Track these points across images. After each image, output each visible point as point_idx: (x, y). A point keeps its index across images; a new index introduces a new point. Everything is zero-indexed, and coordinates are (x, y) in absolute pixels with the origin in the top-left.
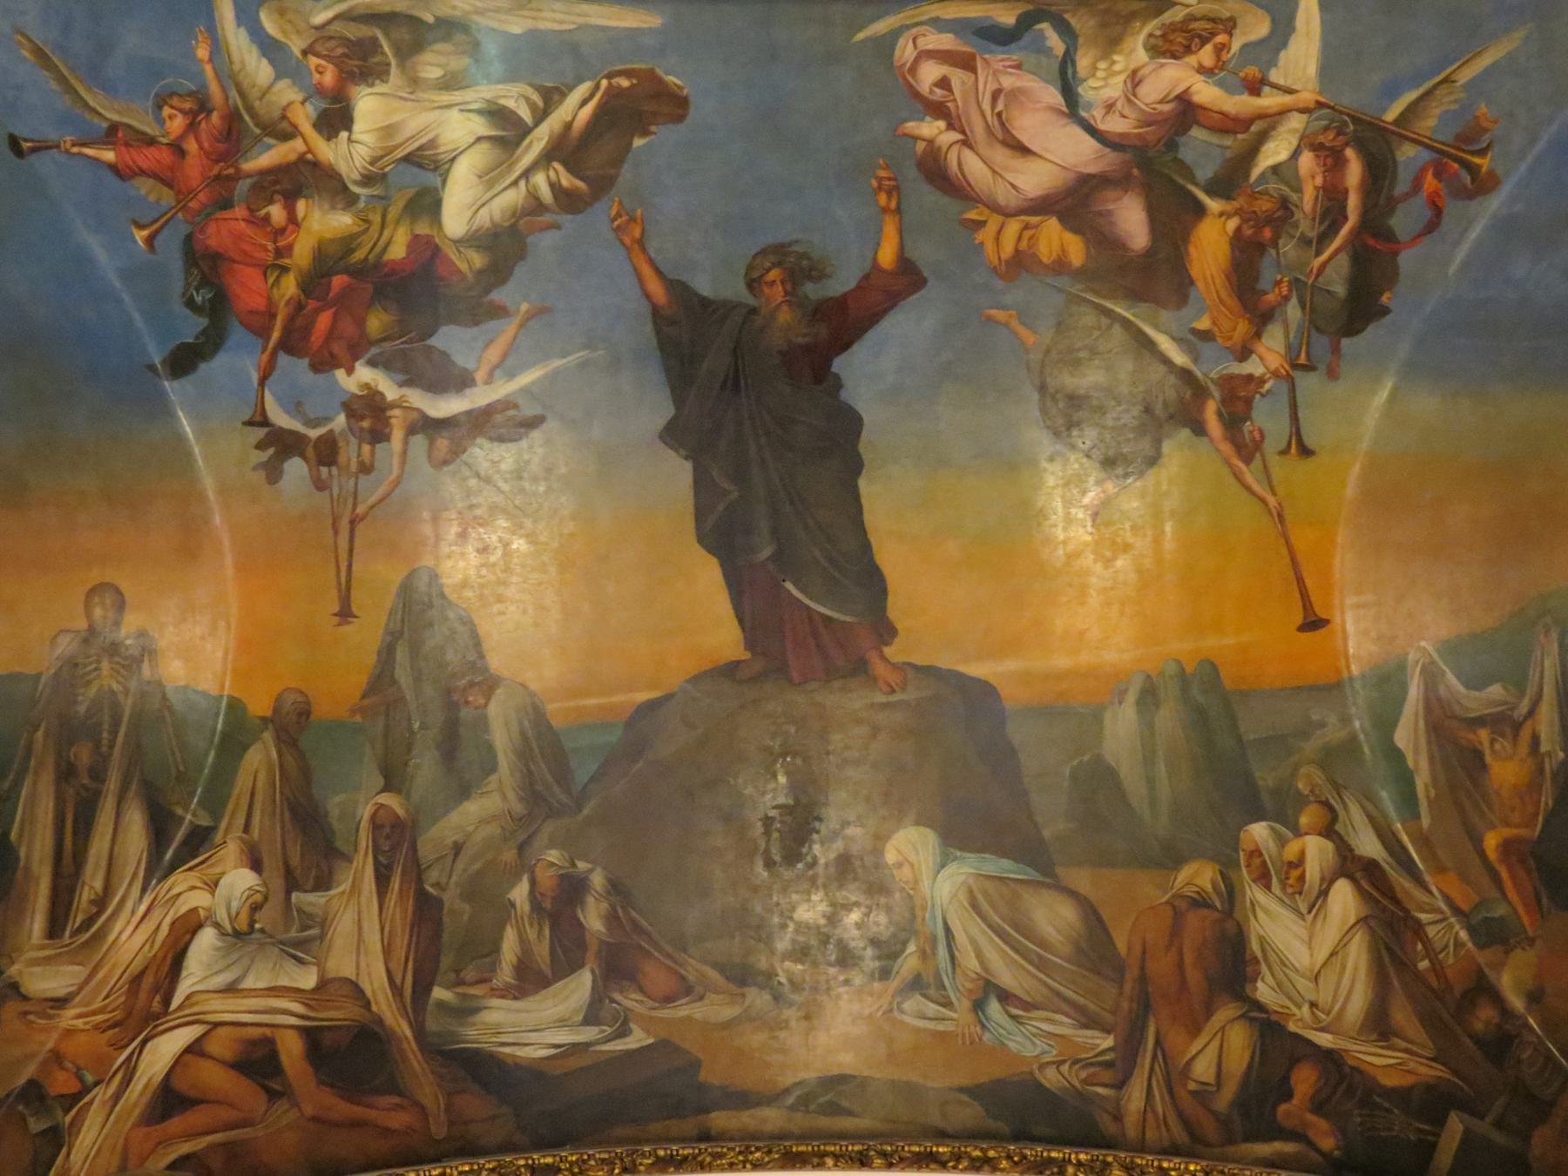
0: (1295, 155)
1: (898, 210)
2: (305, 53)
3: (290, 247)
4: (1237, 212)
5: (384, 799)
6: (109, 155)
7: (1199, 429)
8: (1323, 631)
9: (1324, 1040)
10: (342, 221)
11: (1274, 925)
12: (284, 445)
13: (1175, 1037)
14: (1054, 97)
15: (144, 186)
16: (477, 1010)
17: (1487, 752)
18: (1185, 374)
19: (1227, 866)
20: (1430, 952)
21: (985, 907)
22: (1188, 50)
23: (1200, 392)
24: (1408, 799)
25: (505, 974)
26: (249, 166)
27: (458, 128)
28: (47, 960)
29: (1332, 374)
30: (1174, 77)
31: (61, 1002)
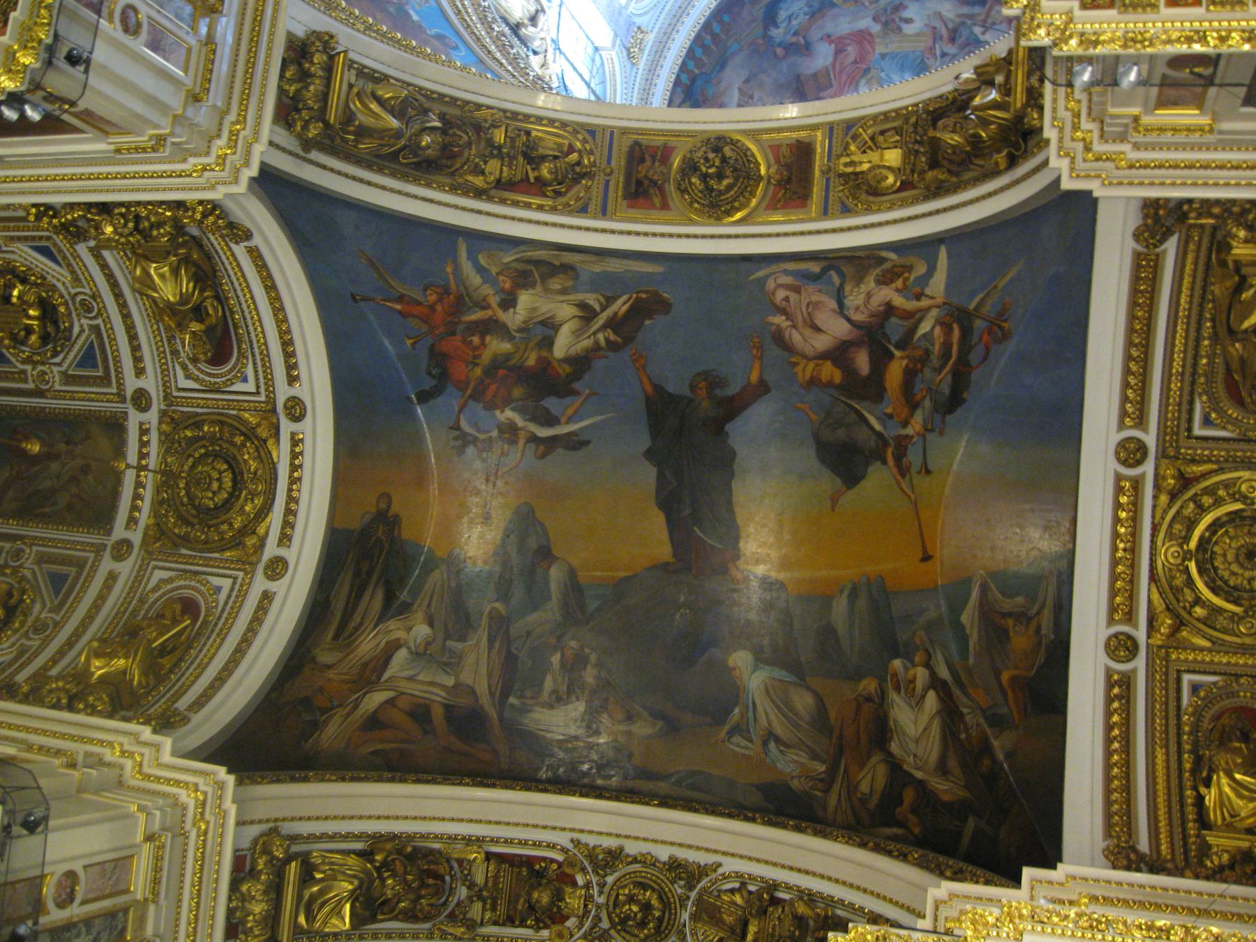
0: (933, 328)
1: (761, 358)
2: (498, 274)
3: (480, 356)
4: (908, 357)
5: (497, 605)
6: (399, 307)
7: (885, 462)
8: (929, 562)
9: (919, 775)
10: (506, 347)
14: (833, 304)
15: (413, 322)
16: (530, 711)
17: (1011, 629)
18: (879, 435)
19: (882, 680)
20: (967, 730)
21: (772, 693)
22: (892, 281)
23: (886, 444)
24: (964, 650)
27: (565, 311)
28: (329, 649)
29: (941, 433)
30: (888, 294)
31: (328, 667)
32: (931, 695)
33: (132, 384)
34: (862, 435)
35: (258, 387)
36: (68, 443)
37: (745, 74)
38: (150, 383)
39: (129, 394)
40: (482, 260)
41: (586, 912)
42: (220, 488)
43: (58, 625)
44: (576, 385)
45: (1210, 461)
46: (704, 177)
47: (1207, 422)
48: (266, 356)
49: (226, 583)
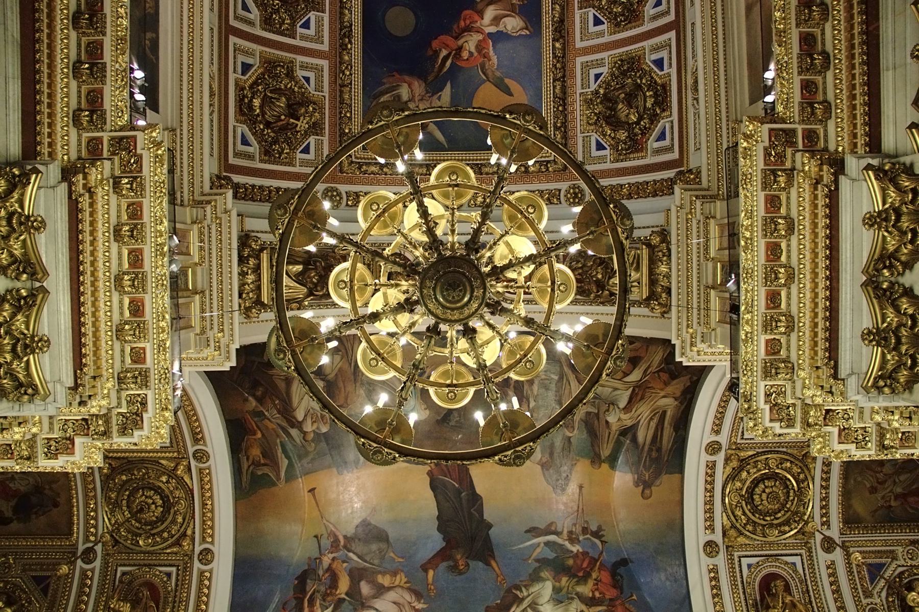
5: (571, 435)
7: (345, 537)
10: (580, 589)
12: (597, 534)
13: (346, 366)
18: (349, 551)
20: (275, 405)
23: (345, 547)
26: (605, 608)
32: (300, 419)
33: (838, 555)
35: (740, 561)
36: (890, 506)
38: (822, 558)
42: (761, 495)
44: (537, 565)
45: (168, 553)
47: (169, 575)
48: (734, 585)
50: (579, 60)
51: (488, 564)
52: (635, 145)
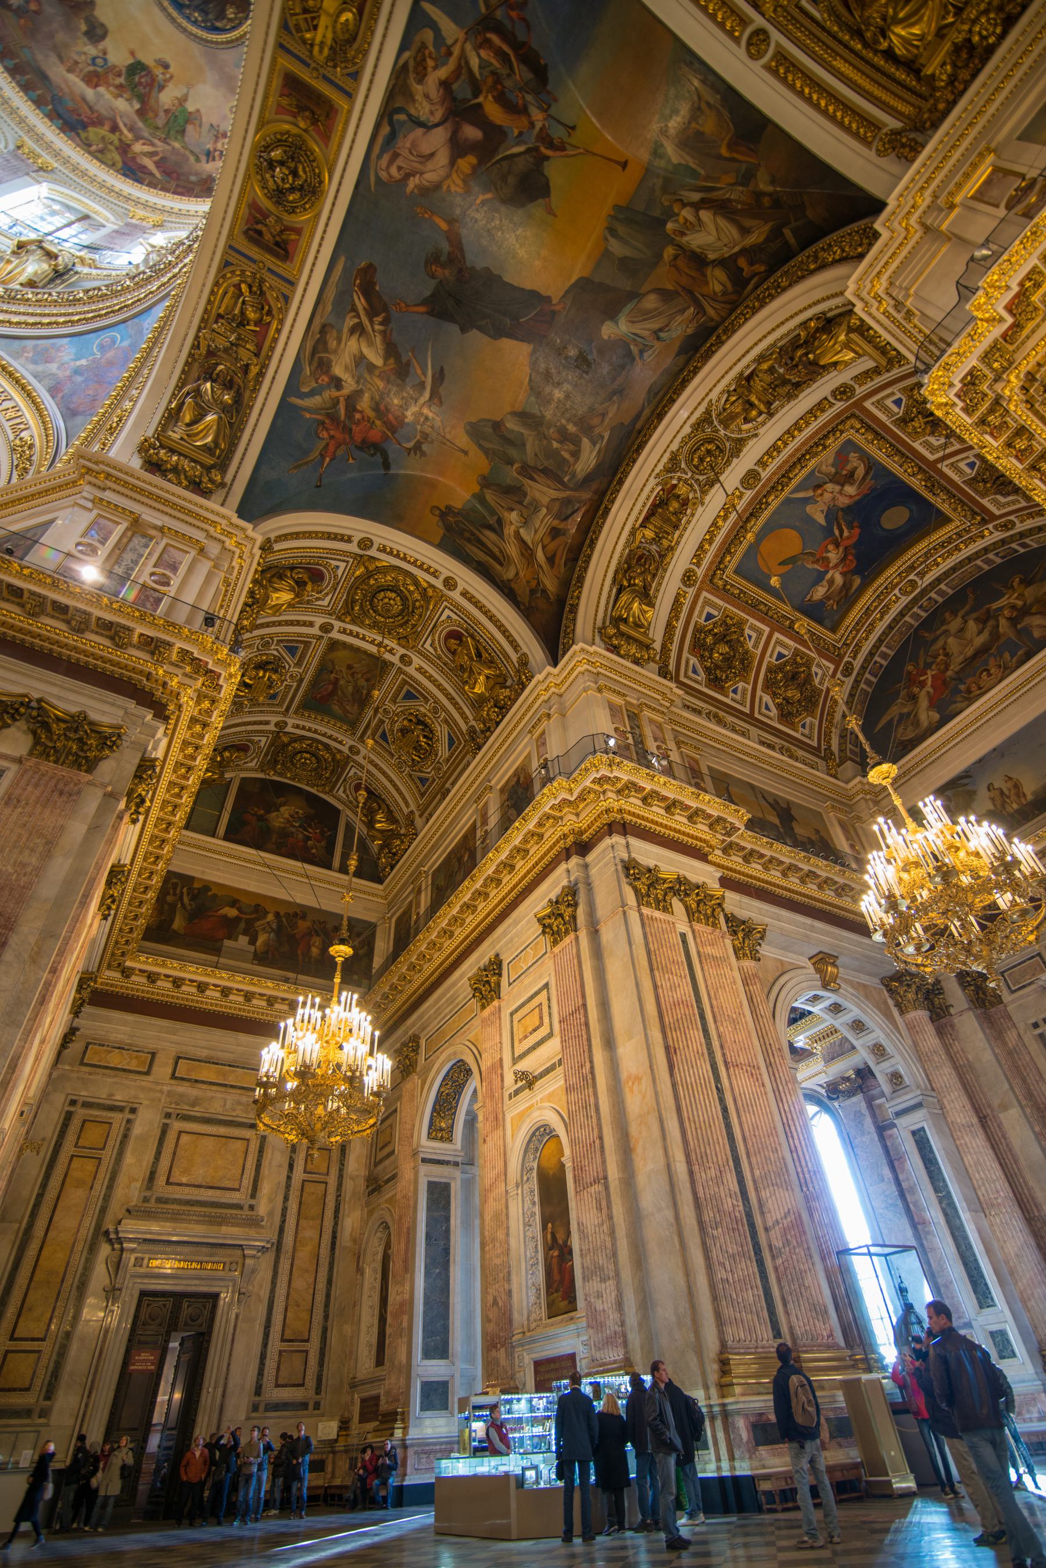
6: (328, 459)
7: (547, 158)
9: (737, 249)
11: (696, 240)
12: (418, 447)
14: (420, 131)
15: (339, 453)
18: (528, 151)
19: (671, 242)
20: (738, 202)
22: (425, 68)
23: (536, 149)
24: (694, 174)
25: (571, 460)
27: (353, 345)
29: (556, 100)
31: (517, 574)
33: (315, 631)
34: (521, 165)
37: (53, 58)
38: (319, 621)
39: (320, 633)
40: (305, 390)
41: (691, 486)
43: (436, 701)
44: (404, 360)
46: (292, 189)
48: (330, 550)
49: (447, 612)
50: (767, 630)
51: (424, 302)
52: (698, 647)
